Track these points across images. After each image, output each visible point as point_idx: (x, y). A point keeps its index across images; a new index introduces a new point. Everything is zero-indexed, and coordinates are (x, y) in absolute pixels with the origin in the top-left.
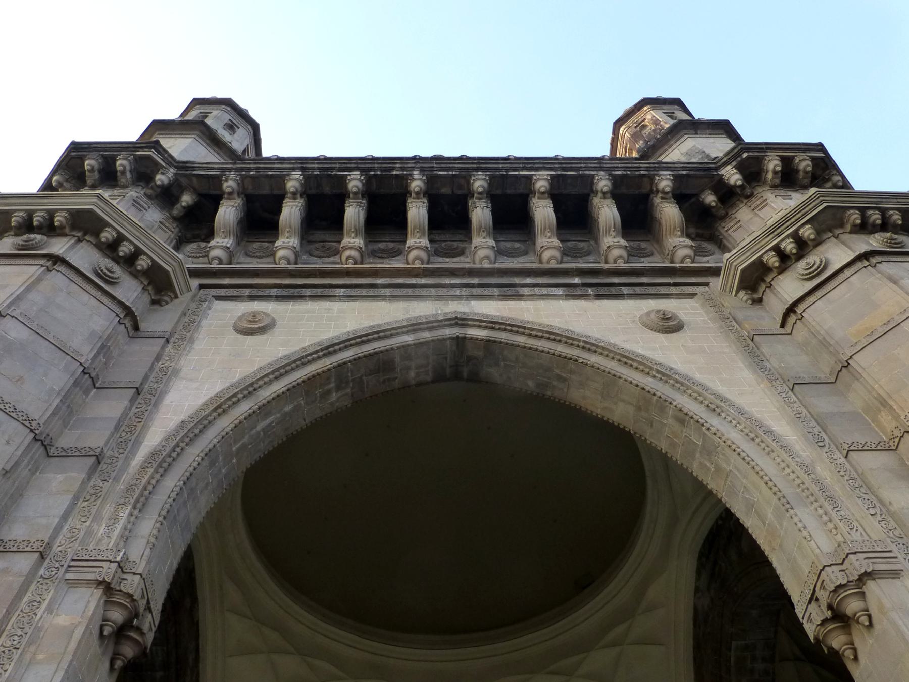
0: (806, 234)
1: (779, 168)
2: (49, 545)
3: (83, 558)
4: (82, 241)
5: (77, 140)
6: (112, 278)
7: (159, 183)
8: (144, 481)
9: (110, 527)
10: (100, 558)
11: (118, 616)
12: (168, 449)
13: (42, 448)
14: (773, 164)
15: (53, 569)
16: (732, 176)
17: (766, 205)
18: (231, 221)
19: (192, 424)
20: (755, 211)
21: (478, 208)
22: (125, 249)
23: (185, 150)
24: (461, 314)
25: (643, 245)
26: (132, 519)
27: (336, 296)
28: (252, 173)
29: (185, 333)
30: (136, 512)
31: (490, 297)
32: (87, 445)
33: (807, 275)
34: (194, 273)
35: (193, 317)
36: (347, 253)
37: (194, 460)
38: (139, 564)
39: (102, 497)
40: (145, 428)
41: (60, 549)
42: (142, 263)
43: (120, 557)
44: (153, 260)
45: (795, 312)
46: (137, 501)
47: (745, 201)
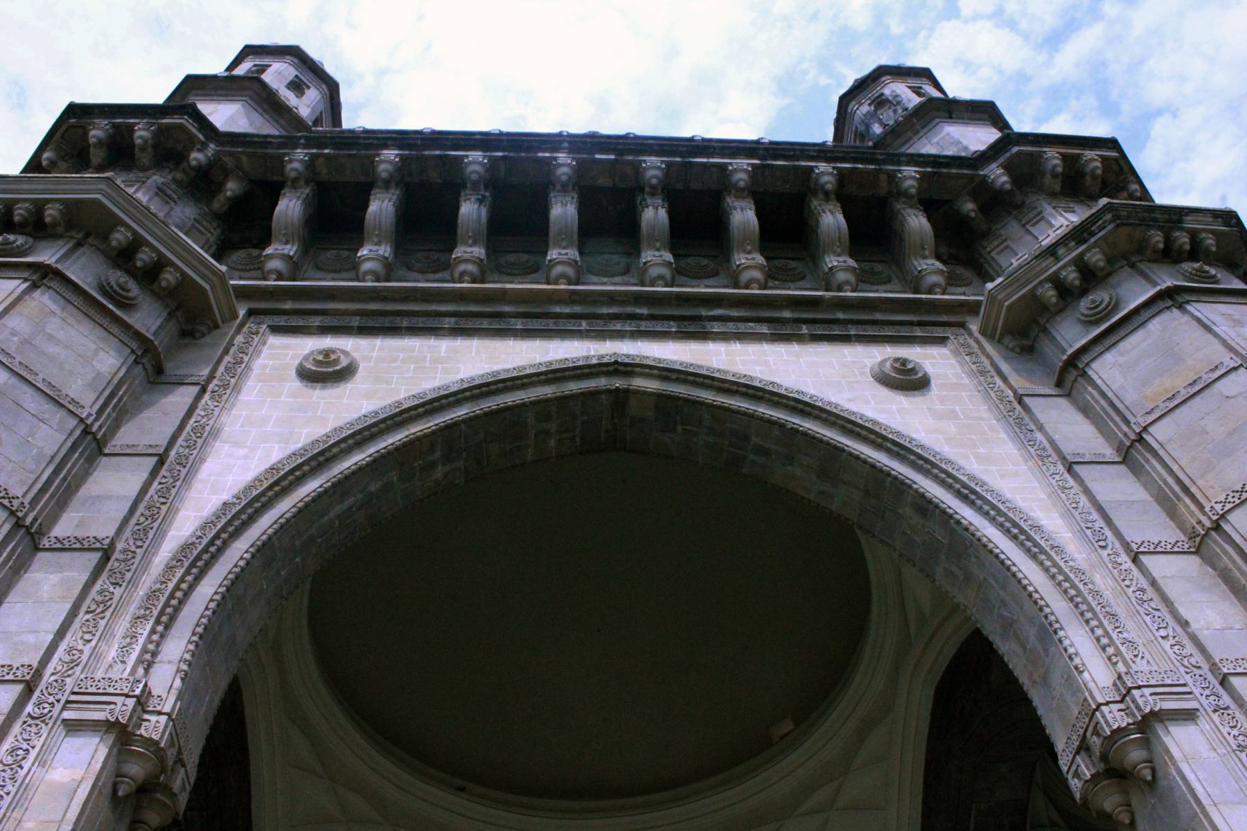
0: (1094, 259)
2: (38, 673)
3: (87, 691)
4: (83, 246)
5: (79, 100)
6: (126, 298)
7: (194, 163)
8: (171, 586)
9: (125, 650)
10: (111, 690)
11: (136, 770)
12: (205, 541)
13: (28, 538)
15: (46, 705)
16: (996, 174)
17: (1043, 218)
18: (296, 220)
19: (238, 508)
20: (1028, 226)
22: (144, 257)
23: (232, 118)
26: (155, 637)
27: (444, 328)
28: (327, 151)
29: (228, 378)
30: (160, 628)
32: (91, 534)
34: (244, 294)
35: (241, 355)
37: (242, 558)
38: (166, 699)
39: (113, 606)
40: (172, 512)
41: (53, 678)
42: (168, 278)
43: (140, 689)
45: (1076, 367)
46: (162, 613)
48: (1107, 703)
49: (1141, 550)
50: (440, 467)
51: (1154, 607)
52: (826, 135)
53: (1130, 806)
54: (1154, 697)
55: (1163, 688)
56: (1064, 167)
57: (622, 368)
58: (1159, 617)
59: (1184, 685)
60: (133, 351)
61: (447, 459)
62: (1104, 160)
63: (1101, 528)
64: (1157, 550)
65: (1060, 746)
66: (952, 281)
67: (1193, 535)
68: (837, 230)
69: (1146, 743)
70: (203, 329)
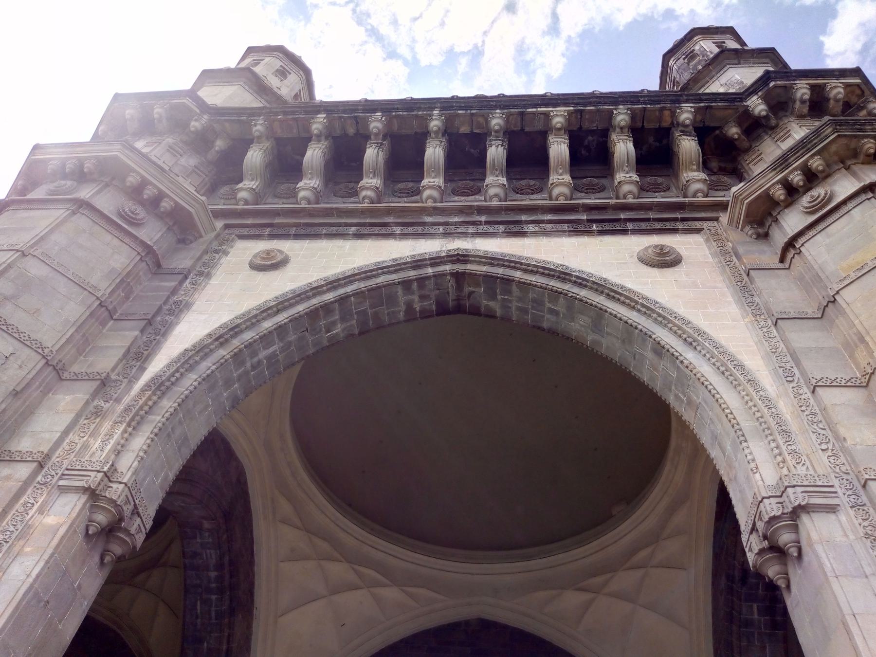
0: (815, 165)
1: (807, 97)
2: (48, 456)
3: (76, 468)
4: (109, 186)
5: (120, 92)
6: (136, 219)
7: (192, 129)
8: (141, 402)
9: (104, 442)
10: (90, 468)
11: (101, 518)
12: (168, 374)
13: (54, 373)
14: (802, 90)
15: (49, 477)
16: (757, 105)
17: (789, 136)
19: (193, 352)
20: (778, 143)
21: (494, 147)
24: (464, 251)
25: (660, 180)
26: (126, 435)
27: (349, 234)
28: (279, 117)
29: (203, 269)
30: (130, 429)
31: (493, 235)
32: (95, 370)
33: (810, 208)
34: (218, 214)
35: (214, 255)
36: (364, 193)
37: (192, 385)
38: (126, 474)
39: (102, 415)
41: (58, 459)
42: (166, 205)
43: (107, 468)
44: (176, 203)
45: (794, 247)
46: (132, 419)
47: (770, 132)
48: (769, 497)
49: (818, 384)
50: (339, 326)
51: (822, 427)
52: (654, 85)
53: (787, 574)
54: (804, 494)
55: (812, 488)
56: (811, 94)
57: (461, 258)
58: (824, 435)
59: (832, 486)
60: (139, 254)
61: (343, 319)
62: (847, 86)
63: (792, 367)
64: (833, 384)
65: (742, 528)
66: (713, 186)
67: (864, 373)
68: (626, 154)
69: (795, 528)
70: (190, 237)
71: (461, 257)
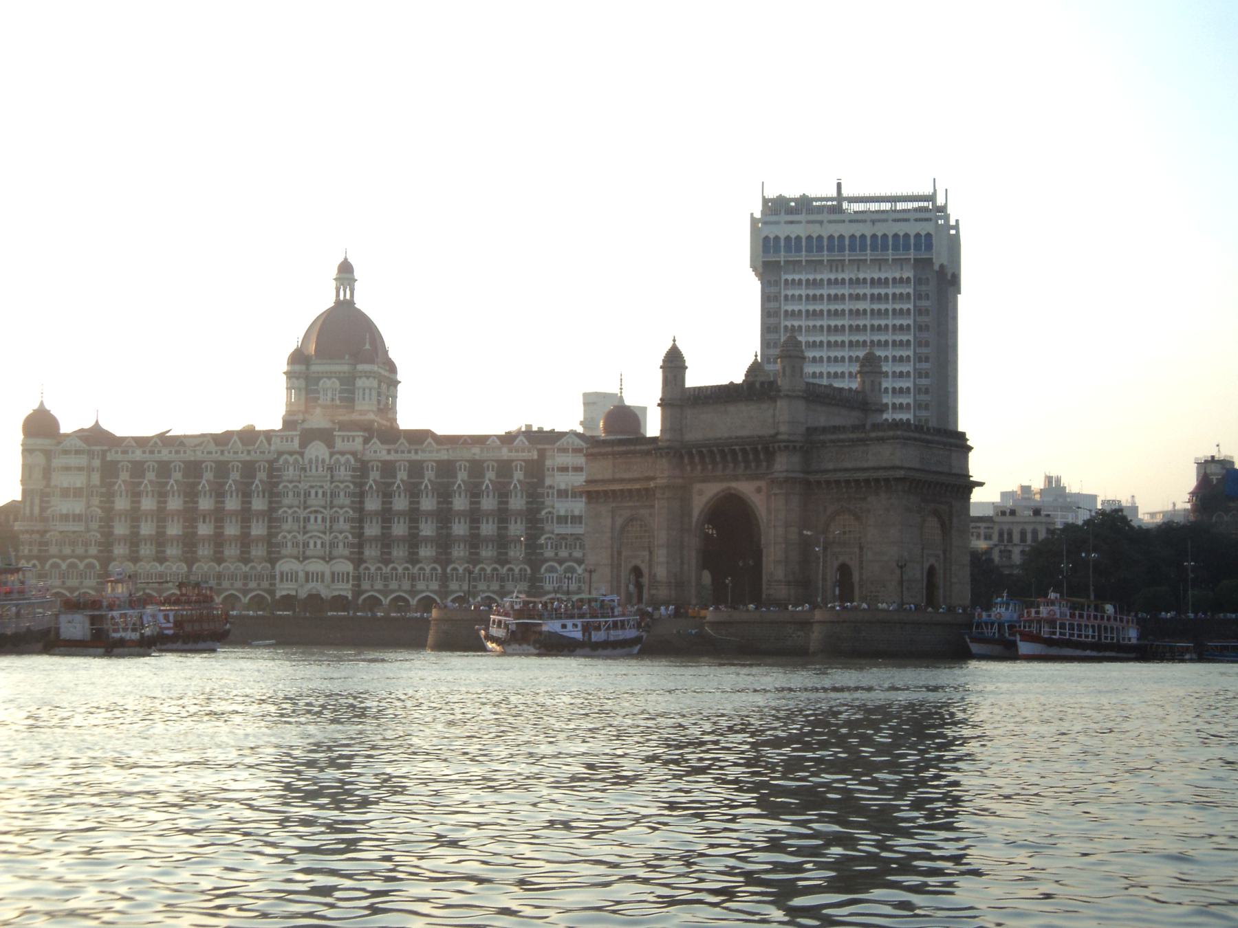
71: (729, 488)
